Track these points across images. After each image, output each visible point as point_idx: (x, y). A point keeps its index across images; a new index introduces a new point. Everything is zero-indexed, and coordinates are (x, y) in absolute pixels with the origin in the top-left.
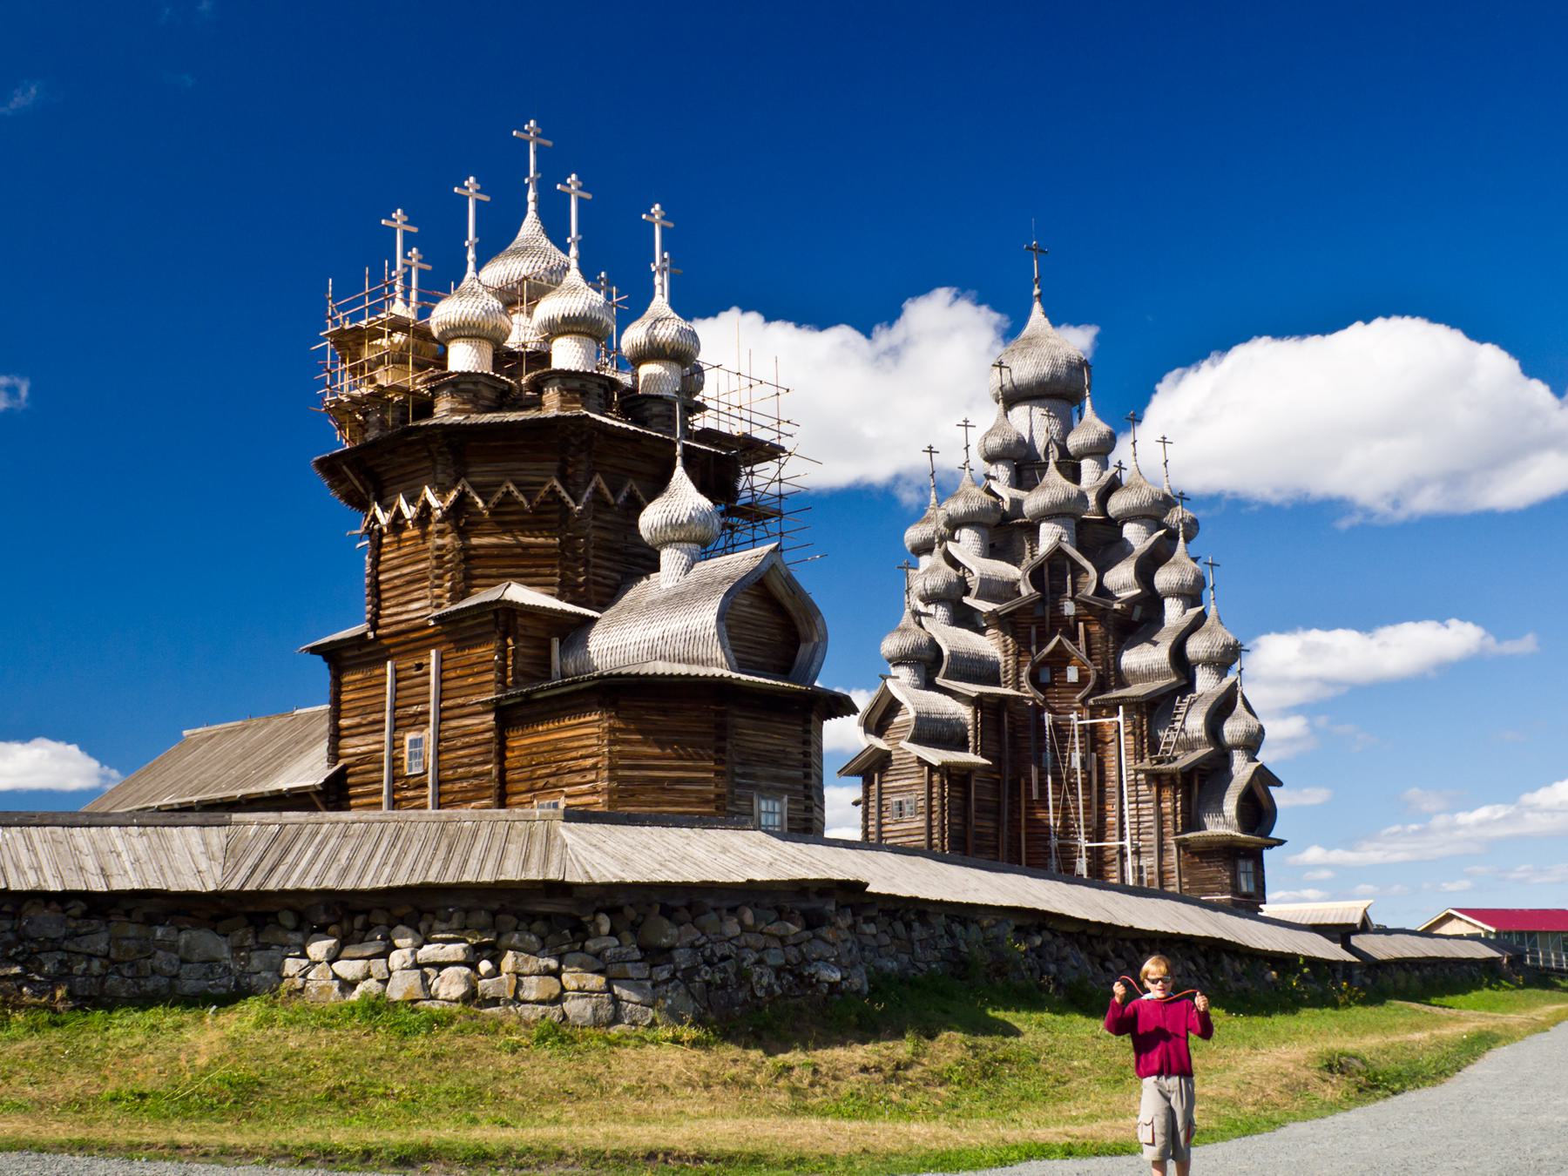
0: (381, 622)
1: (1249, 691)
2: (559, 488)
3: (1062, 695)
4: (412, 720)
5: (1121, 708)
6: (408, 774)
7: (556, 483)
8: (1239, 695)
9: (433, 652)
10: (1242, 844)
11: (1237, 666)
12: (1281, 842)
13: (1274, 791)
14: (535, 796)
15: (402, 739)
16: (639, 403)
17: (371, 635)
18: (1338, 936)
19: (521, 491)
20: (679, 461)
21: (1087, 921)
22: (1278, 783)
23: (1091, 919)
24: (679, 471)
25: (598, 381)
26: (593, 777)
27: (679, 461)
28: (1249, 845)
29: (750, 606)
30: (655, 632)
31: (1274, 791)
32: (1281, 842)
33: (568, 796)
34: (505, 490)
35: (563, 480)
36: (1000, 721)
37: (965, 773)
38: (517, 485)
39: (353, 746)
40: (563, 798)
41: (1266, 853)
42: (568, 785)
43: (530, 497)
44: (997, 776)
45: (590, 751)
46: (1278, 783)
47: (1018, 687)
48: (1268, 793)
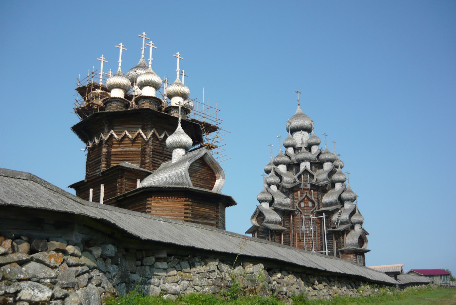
1: (359, 208)
3: (308, 210)
5: (324, 214)
8: (357, 209)
10: (358, 251)
11: (355, 201)
12: (369, 251)
13: (367, 236)
16: (170, 109)
18: (394, 276)
20: (179, 124)
21: (304, 267)
22: (368, 234)
23: (306, 266)
24: (179, 127)
25: (155, 100)
27: (179, 124)
29: (199, 167)
30: (167, 175)
31: (367, 236)
32: (369, 251)
34: (125, 133)
37: (280, 232)
41: (365, 254)
44: (290, 233)
46: (368, 234)
47: (293, 207)
48: (365, 237)
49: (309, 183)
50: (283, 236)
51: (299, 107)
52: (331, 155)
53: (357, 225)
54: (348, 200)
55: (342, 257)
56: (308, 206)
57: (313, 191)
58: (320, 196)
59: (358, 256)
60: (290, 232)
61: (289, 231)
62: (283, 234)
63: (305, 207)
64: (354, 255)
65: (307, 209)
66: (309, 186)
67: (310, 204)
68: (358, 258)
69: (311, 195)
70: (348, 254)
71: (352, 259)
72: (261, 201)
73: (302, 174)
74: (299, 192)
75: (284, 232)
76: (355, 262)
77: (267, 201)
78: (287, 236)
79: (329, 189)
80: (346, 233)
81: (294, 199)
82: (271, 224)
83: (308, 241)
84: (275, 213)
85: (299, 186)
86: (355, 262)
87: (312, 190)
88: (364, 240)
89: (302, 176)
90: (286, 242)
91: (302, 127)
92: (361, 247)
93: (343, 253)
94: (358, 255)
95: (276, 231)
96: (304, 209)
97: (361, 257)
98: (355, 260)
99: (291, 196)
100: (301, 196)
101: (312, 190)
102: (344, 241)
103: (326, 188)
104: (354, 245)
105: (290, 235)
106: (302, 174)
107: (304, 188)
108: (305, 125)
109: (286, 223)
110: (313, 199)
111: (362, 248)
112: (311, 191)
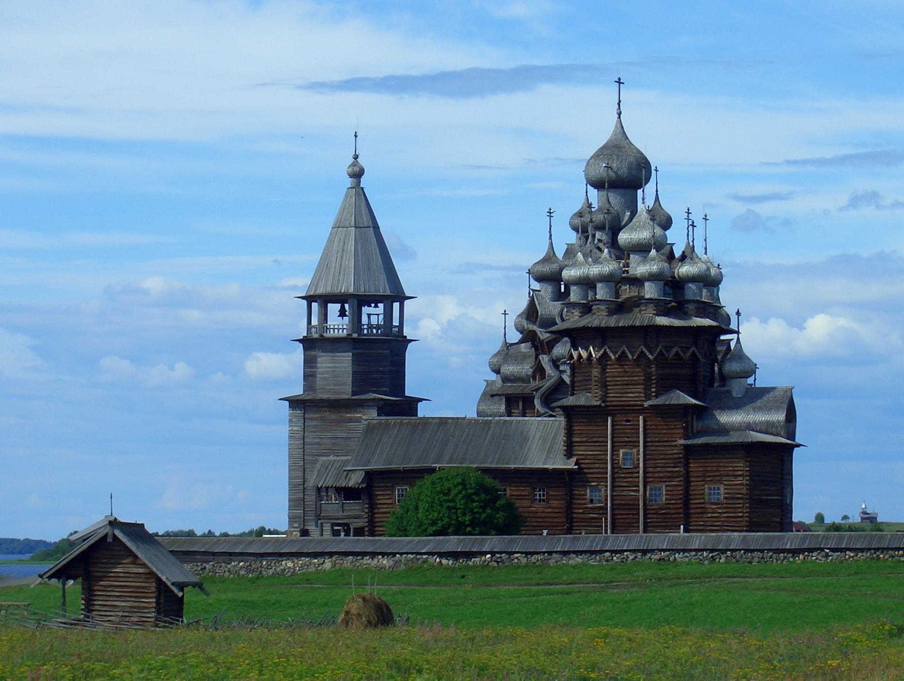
0: (608, 399)
2: (696, 351)
4: (624, 444)
6: (623, 467)
7: (694, 348)
9: (641, 417)
14: (706, 484)
15: (619, 451)
17: (603, 405)
19: (681, 351)
26: (742, 479)
33: (725, 485)
35: (696, 345)
38: (680, 347)
39: (579, 451)
40: (722, 486)
42: (726, 481)
43: (684, 353)
45: (739, 468)
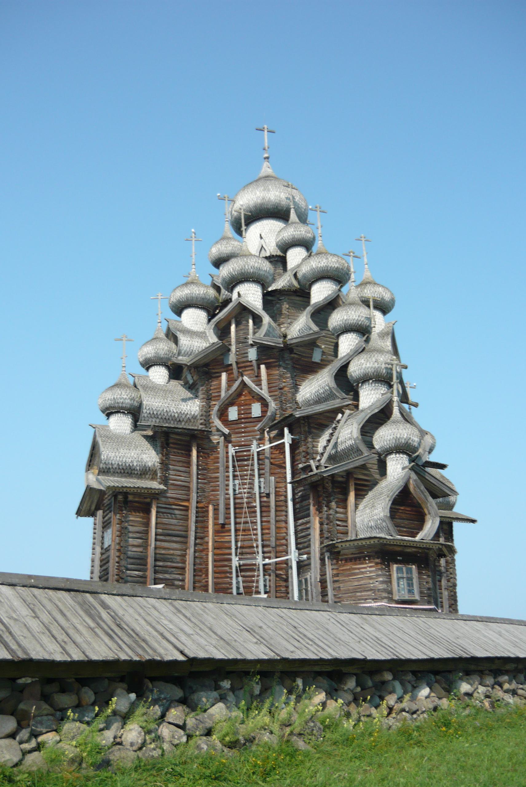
28: (409, 550)
36: (189, 456)
37: (148, 500)
49: (252, 345)
50: (157, 512)
51: (266, 164)
52: (327, 258)
53: (393, 456)
54: (365, 379)
55: (335, 572)
56: (249, 416)
57: (267, 368)
58: (290, 381)
59: (395, 567)
60: (188, 500)
61: (184, 497)
62: (158, 507)
63: (239, 419)
64: (377, 564)
65: (247, 424)
66: (252, 354)
67: (256, 410)
68: (395, 575)
69: (258, 383)
70: (355, 559)
71: (370, 578)
72: (109, 412)
73: (233, 321)
74: (224, 376)
75: (163, 499)
76: (381, 587)
77: (122, 408)
78: (177, 512)
79: (322, 360)
80: (356, 490)
81: (209, 398)
82: (125, 477)
83: (242, 526)
84: (149, 446)
85: (223, 360)
86: (381, 587)
87: (263, 367)
88: (426, 511)
89: (233, 328)
90: (170, 532)
91: (261, 205)
92: (414, 537)
93: (338, 560)
94: (398, 562)
95: (130, 498)
96: (239, 426)
97: (409, 571)
98: (382, 582)
99: (202, 390)
100: (229, 386)
101: (263, 367)
102: (347, 518)
103: (311, 357)
104: (377, 527)
105: (187, 509)
106: (233, 321)
107: (237, 363)
108: (269, 200)
109: (171, 472)
110: (264, 392)
111: (418, 538)
112: (259, 368)
